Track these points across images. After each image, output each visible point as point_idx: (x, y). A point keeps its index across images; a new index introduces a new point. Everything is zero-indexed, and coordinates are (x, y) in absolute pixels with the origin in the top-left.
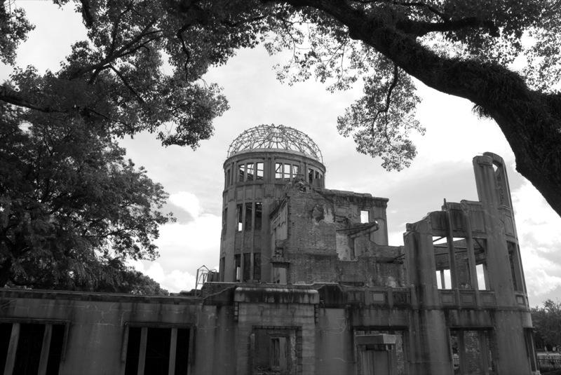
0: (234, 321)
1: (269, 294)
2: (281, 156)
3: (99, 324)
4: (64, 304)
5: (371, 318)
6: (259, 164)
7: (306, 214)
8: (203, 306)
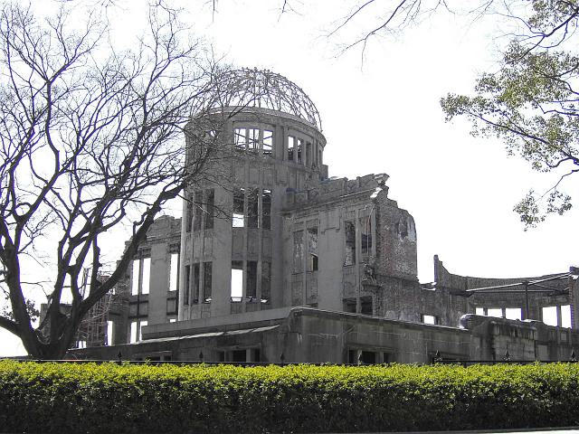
7: (394, 228)
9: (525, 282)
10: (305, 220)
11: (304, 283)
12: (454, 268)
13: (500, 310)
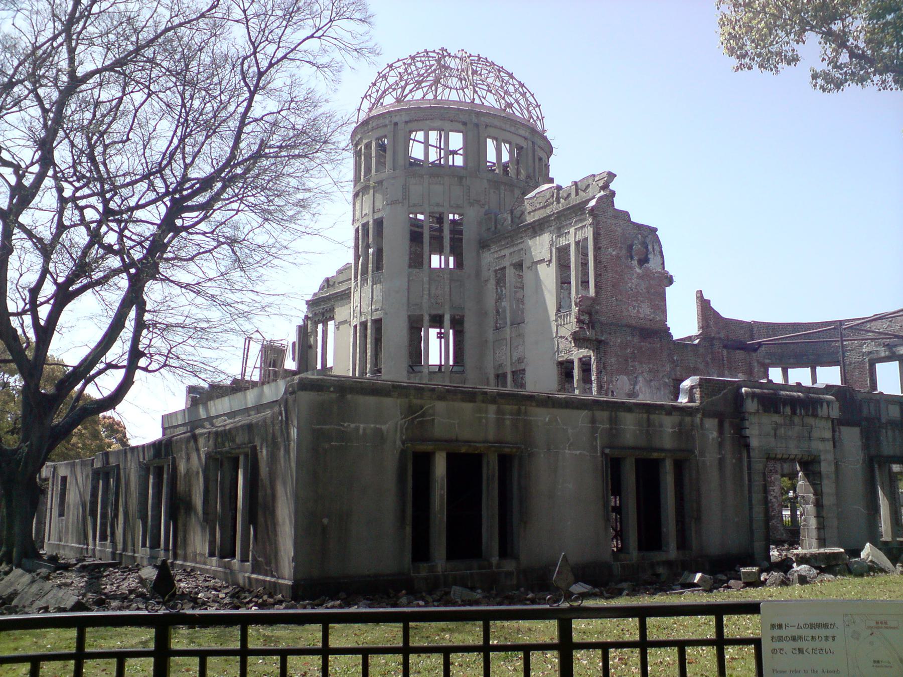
2: (496, 122)
3: (567, 451)
4: (511, 414)
8: (702, 420)
10: (506, 252)
11: (508, 340)
12: (728, 309)
13: (808, 370)
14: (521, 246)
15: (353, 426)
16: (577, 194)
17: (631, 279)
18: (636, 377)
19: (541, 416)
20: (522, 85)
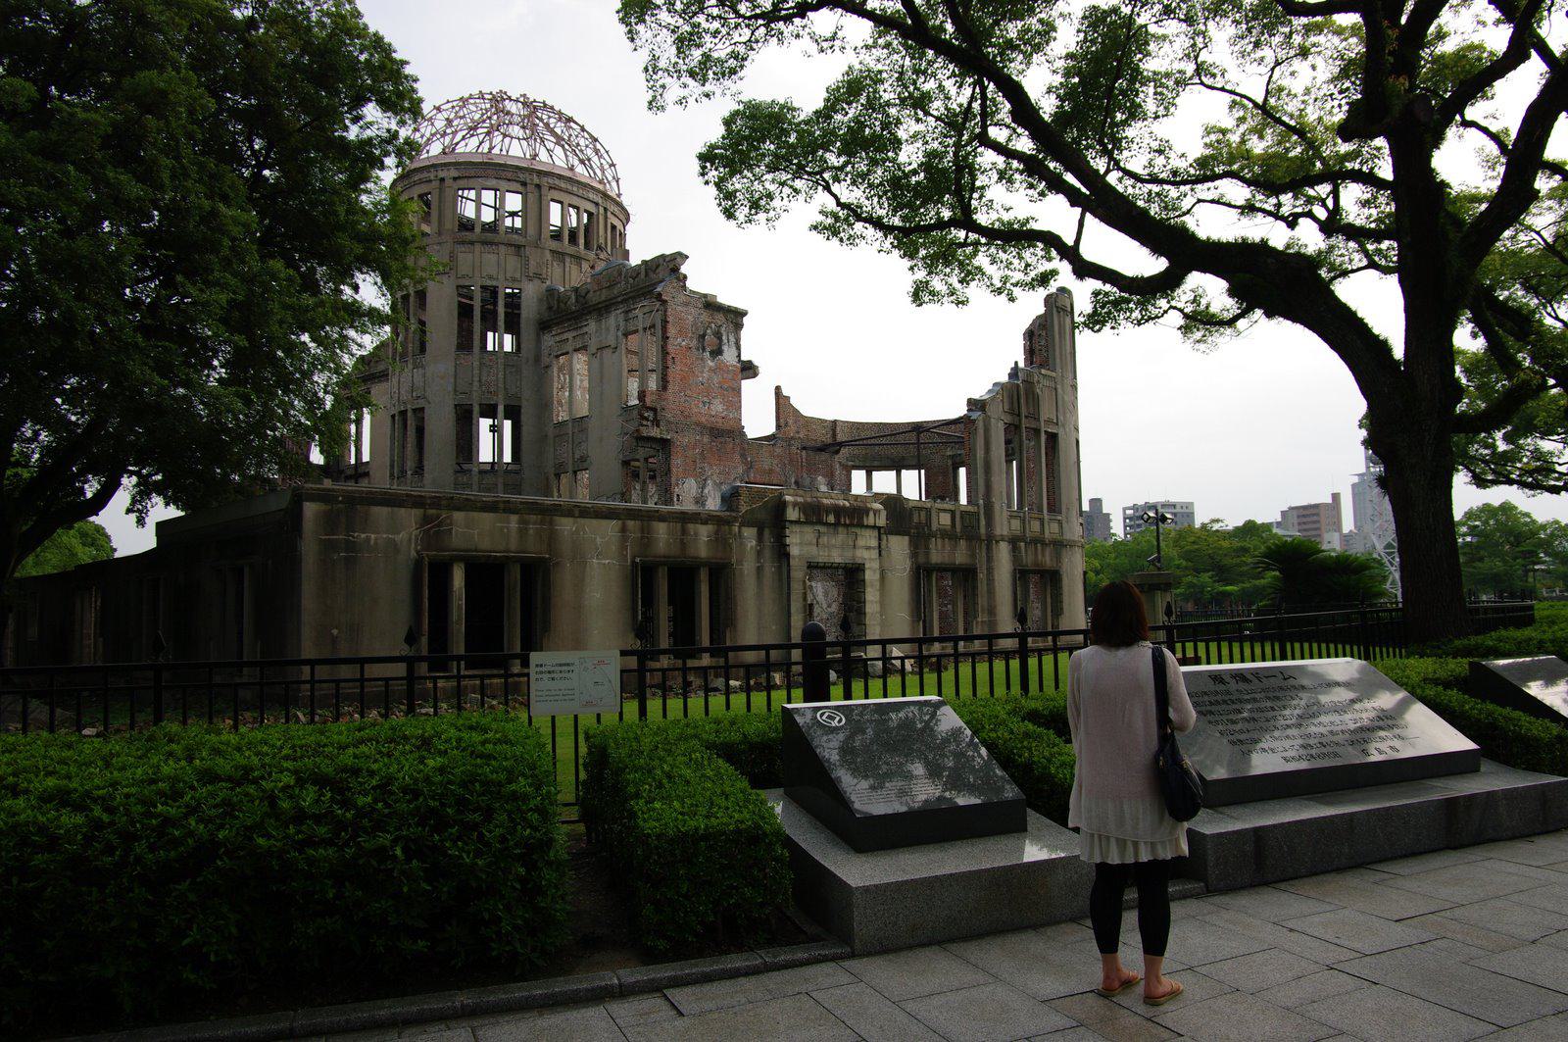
0: (782, 554)
1: (829, 510)
2: (563, 185)
4: (535, 523)
5: (938, 553)
6: (484, 193)
7: (695, 342)
8: (740, 527)
9: (918, 428)
10: (569, 335)
13: (893, 473)
14: (585, 329)
15: (363, 536)
16: (647, 275)
17: (702, 372)
18: (705, 480)
19: (566, 526)
20: (596, 140)
